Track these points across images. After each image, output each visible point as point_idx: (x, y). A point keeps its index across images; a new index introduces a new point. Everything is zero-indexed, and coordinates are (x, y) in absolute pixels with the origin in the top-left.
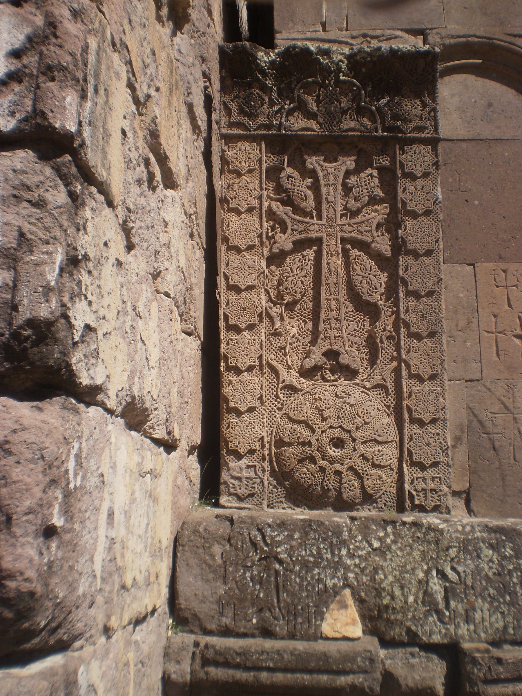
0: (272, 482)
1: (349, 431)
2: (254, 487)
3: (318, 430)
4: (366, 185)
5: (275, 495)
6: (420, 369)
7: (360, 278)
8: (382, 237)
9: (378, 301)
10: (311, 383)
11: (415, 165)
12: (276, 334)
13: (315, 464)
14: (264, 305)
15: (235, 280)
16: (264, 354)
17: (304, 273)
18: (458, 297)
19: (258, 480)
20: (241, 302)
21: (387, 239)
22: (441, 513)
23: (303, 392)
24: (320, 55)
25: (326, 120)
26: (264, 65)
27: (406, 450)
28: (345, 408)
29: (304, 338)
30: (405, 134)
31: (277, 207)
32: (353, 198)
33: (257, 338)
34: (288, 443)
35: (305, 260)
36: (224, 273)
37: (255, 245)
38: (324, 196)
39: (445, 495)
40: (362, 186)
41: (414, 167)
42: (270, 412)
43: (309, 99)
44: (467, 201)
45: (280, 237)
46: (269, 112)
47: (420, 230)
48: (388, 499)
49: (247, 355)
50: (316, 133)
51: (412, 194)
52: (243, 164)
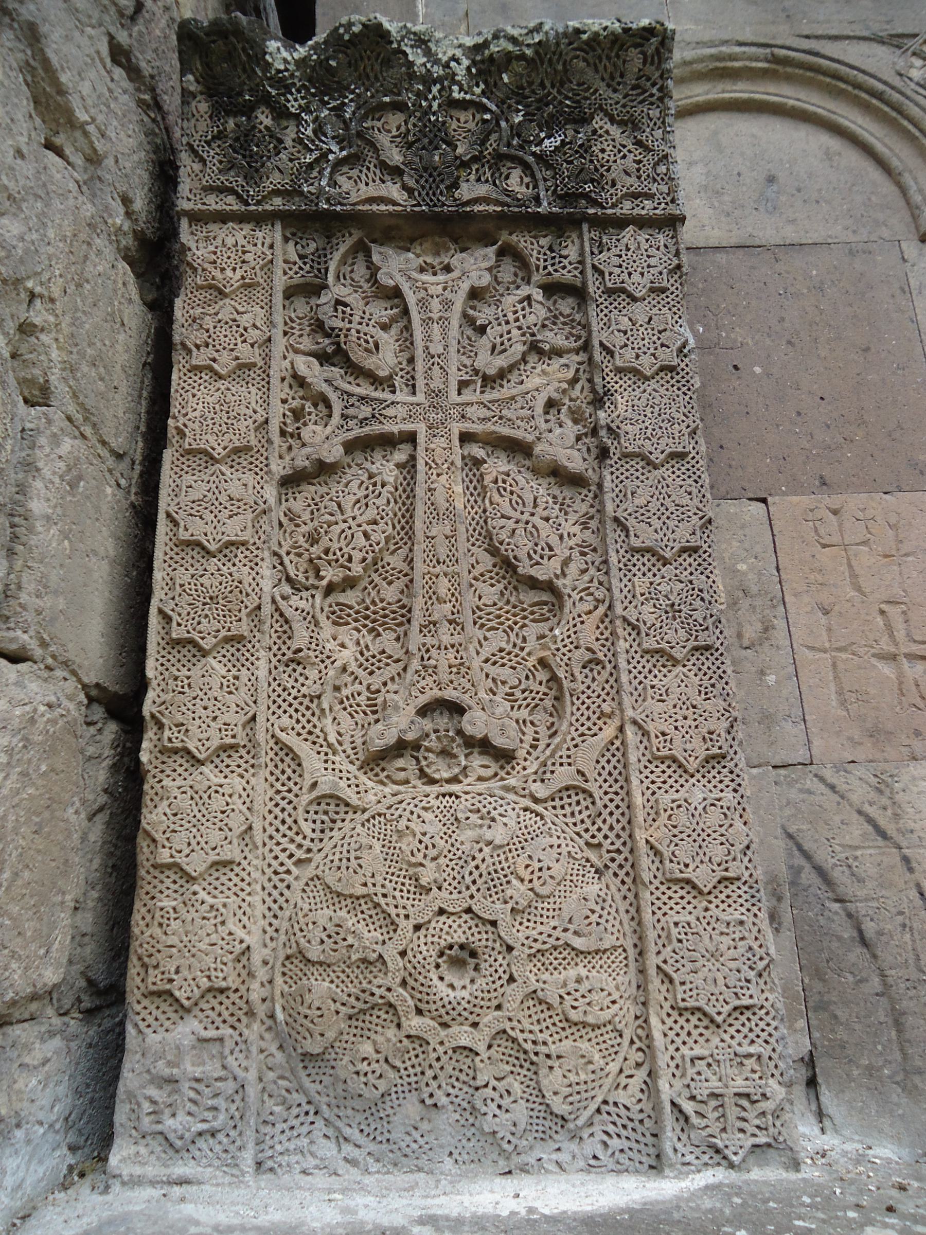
0: (271, 1087)
1: (494, 923)
2: (215, 1109)
3: (402, 922)
4: (517, 320)
6: (678, 742)
7: (511, 524)
8: (558, 431)
9: (557, 576)
11: (630, 274)
12: (296, 661)
13: (399, 1026)
15: (196, 529)
17: (371, 513)
19: (229, 1087)
23: (366, 815)
26: (282, 67)
27: (652, 971)
28: (479, 856)
29: (371, 673)
31: (308, 368)
32: (490, 345)
33: (244, 670)
34: (321, 964)
35: (375, 484)
36: (168, 515)
40: (507, 323)
41: (625, 276)
42: (276, 873)
43: (383, 140)
45: (313, 432)
47: (649, 410)
48: (611, 1128)
49: (215, 718)
50: (401, 208)
51: (625, 333)
52: (229, 273)
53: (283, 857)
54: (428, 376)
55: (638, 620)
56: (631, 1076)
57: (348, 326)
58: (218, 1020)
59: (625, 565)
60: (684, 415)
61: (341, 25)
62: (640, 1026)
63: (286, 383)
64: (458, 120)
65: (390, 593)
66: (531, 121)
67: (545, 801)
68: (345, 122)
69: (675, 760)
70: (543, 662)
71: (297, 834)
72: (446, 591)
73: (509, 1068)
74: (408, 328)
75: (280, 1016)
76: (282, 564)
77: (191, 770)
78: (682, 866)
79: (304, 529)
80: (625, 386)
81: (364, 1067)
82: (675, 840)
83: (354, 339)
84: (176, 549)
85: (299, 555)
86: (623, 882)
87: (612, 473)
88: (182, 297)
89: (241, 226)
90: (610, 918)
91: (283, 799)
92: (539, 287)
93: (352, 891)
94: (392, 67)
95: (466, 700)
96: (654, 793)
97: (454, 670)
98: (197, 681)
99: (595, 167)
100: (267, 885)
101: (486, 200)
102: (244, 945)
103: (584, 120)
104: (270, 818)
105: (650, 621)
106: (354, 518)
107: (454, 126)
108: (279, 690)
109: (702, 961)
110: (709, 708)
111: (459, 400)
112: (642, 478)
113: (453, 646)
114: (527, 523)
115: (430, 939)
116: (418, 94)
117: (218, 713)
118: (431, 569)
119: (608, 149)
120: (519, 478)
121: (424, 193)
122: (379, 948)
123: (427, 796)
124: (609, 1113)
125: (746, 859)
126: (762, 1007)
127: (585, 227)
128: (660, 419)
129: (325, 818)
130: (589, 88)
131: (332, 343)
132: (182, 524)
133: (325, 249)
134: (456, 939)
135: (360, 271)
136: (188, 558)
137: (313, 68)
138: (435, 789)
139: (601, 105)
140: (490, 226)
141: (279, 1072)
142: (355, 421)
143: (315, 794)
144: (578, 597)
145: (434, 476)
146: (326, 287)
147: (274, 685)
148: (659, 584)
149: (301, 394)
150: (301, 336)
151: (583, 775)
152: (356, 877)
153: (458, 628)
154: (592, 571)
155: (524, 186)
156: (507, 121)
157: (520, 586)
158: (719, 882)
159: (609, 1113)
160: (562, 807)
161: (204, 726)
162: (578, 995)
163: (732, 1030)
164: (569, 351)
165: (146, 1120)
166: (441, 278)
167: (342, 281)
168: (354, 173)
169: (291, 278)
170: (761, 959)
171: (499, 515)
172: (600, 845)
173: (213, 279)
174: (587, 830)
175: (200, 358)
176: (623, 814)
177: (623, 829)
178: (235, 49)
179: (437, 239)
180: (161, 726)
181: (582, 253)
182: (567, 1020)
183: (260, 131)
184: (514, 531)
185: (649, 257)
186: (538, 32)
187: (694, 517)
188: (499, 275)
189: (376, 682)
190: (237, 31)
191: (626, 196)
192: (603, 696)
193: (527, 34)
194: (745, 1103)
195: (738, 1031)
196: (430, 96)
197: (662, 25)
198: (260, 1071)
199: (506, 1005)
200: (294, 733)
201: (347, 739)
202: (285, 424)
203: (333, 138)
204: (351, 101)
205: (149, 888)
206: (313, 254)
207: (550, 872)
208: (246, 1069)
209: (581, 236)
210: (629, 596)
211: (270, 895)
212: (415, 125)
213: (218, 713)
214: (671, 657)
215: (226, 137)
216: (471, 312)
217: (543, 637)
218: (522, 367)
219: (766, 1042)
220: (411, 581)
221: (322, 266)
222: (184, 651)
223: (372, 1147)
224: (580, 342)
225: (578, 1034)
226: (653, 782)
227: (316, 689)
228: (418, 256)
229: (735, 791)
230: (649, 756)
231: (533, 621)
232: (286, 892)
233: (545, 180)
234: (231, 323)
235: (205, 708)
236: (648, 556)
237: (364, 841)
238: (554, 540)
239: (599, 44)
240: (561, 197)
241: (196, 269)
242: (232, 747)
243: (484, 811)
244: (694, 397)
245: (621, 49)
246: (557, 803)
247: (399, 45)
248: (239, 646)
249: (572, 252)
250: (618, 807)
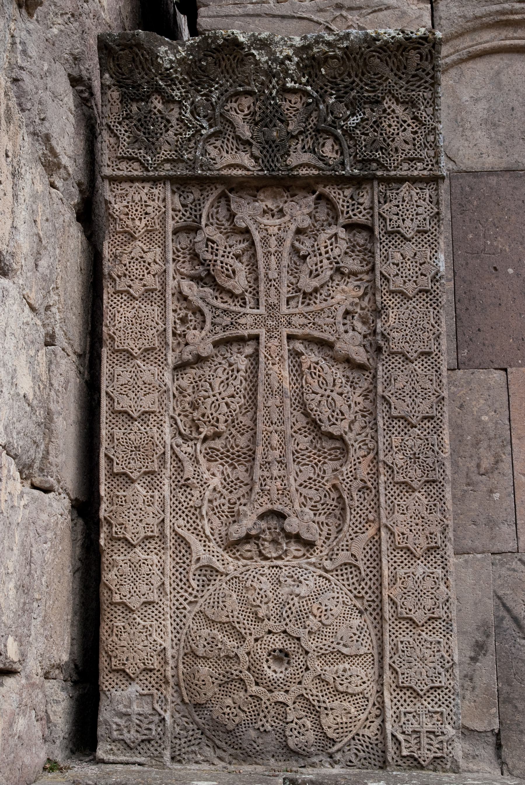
1: (298, 639)
3: (248, 638)
5: (183, 740)
6: (410, 539)
7: (318, 397)
8: (351, 333)
9: (346, 433)
10: (240, 563)
11: (404, 220)
13: (246, 691)
14: (168, 442)
16: (168, 518)
17: (231, 390)
18: (479, 421)
19: (156, 719)
20: (132, 437)
21: (360, 338)
22: (445, 771)
23: (228, 578)
24: (254, 49)
25: (265, 153)
26: (168, 66)
27: (387, 667)
28: (292, 603)
29: (231, 492)
30: (388, 170)
32: (308, 271)
34: (204, 658)
35: (233, 371)
36: (107, 393)
37: (155, 349)
38: (262, 271)
39: (450, 742)
40: (320, 254)
41: (400, 222)
42: (178, 609)
43: (238, 118)
44: (495, 269)
46: (177, 141)
47: (409, 321)
48: (360, 747)
49: (141, 521)
50: (250, 173)
51: (397, 265)
52: (137, 222)
53: (181, 600)
54: (268, 295)
56: (373, 722)
57: (215, 258)
58: (150, 686)
60: (432, 326)
61: (209, 37)
62: (379, 697)
64: (290, 101)
65: (242, 441)
66: (341, 102)
67: (332, 571)
68: (212, 104)
69: (409, 550)
70: (334, 486)
71: (189, 587)
72: (276, 442)
73: (304, 714)
74: (254, 255)
75: (182, 684)
76: (176, 423)
77: (129, 550)
78: (408, 611)
79: (189, 399)
80: (396, 302)
81: (227, 710)
82: (405, 596)
83: (219, 268)
84: (113, 415)
85: (186, 416)
86: (375, 619)
87: (383, 365)
88: (107, 237)
89: (143, 185)
90: (365, 638)
91: (181, 567)
92: (343, 227)
93: (220, 620)
94: (245, 65)
95: (286, 510)
96: (395, 568)
97: (280, 492)
98: (130, 498)
99: (384, 139)
100: (173, 615)
101: (308, 166)
102: (162, 647)
103: (378, 102)
104: (173, 578)
105: (400, 463)
106: (220, 394)
107: (287, 107)
108: (177, 503)
109: (414, 663)
110: (431, 518)
111: (287, 312)
112: (402, 368)
113: (280, 477)
114: (328, 396)
115: (263, 646)
116: (262, 84)
117: (142, 518)
119: (393, 124)
120: (325, 366)
121: (266, 161)
122: (235, 650)
123: (263, 567)
124: (359, 740)
125: (445, 608)
126: (447, 688)
127: (375, 183)
128: (416, 328)
129: (204, 578)
130: (382, 76)
131: (205, 270)
132: (116, 400)
134: (277, 646)
135: (223, 213)
136: (120, 421)
137: (190, 65)
138: (267, 563)
139: (390, 91)
140: (312, 182)
141: (182, 714)
142: (220, 327)
143: (198, 565)
145: (270, 366)
146: (200, 228)
147: (174, 500)
149: (185, 306)
151: (355, 557)
152: (222, 612)
153: (283, 466)
154: (368, 430)
155: (334, 153)
156: (324, 102)
157: (324, 438)
158: (429, 620)
159: (359, 740)
160: (342, 575)
161: (135, 525)
162: (344, 678)
163: (429, 700)
164: (361, 273)
165: (115, 733)
166: (278, 221)
167: (211, 220)
168: (218, 143)
169: (177, 222)
170: (448, 662)
172: (363, 597)
173: (127, 226)
174: (355, 589)
175: (121, 285)
176: (377, 580)
177: (377, 588)
178: (137, 55)
179: (275, 189)
180: (110, 525)
181: (372, 202)
182: (337, 691)
183: (155, 114)
184: (320, 402)
185: (417, 206)
186: (347, 40)
187: (432, 396)
188: (317, 215)
189: (234, 497)
190: (139, 46)
191: (404, 160)
192: (370, 509)
193: (339, 40)
194: (432, 736)
195: (432, 700)
196: (271, 86)
197: (434, 34)
198: (172, 712)
199: (304, 682)
200: (186, 529)
201: (217, 532)
202: (175, 328)
203: (204, 117)
204: (216, 89)
205: (109, 615)
207: (332, 612)
208: (165, 711)
209: (372, 188)
210: (389, 447)
211: (175, 621)
212: (260, 108)
213: (142, 518)
214: (411, 487)
215: (131, 117)
216: (297, 244)
217: (336, 470)
218: (330, 284)
219: (447, 706)
220: (255, 433)
221: (198, 213)
222: (121, 479)
223: (233, 751)
224: (370, 266)
225: (342, 699)
226: (395, 562)
227: (198, 503)
229: (443, 568)
230: (393, 547)
231: (330, 460)
232: (183, 619)
233: (349, 148)
234: (140, 259)
235: (135, 515)
236: (402, 421)
237: (227, 592)
238: (345, 409)
239: (388, 48)
240: (359, 161)
241: (115, 219)
242: (151, 537)
243: (296, 577)
244: (441, 311)
245: (404, 51)
246: (339, 572)
247: (250, 50)
248: (153, 477)
249: (365, 200)
250: (374, 576)
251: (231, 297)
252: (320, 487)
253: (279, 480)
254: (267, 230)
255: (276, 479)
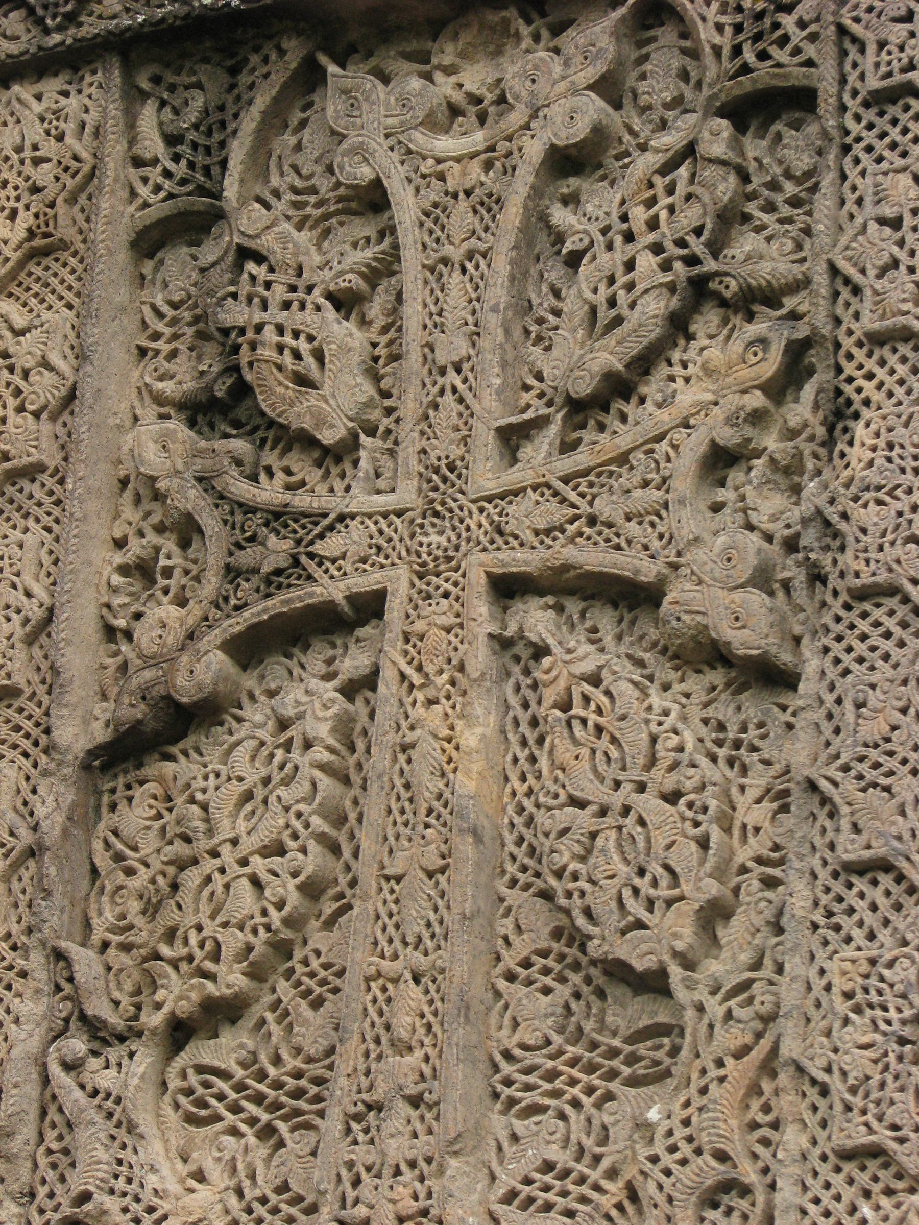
7: (584, 819)
35: (288, 746)
40: (629, 237)
51: (896, 223)
55: (828, 1070)
57: (258, 316)
59: (830, 914)
63: (128, 494)
89: (39, 87)
92: (722, 113)
106: (235, 842)
114: (626, 810)
118: (385, 965)
133: (221, 108)
142: (255, 580)
144: (721, 1011)
146: (219, 215)
148: (890, 965)
149: (155, 519)
150: (173, 354)
171: (563, 797)
184: (593, 835)
206: (196, 126)
228: (449, 71)
231: (633, 1082)
236: (886, 880)
251: (319, 464)
252: (584, 1200)
253: (408, 1175)
254: (442, 177)
255: (398, 1172)
